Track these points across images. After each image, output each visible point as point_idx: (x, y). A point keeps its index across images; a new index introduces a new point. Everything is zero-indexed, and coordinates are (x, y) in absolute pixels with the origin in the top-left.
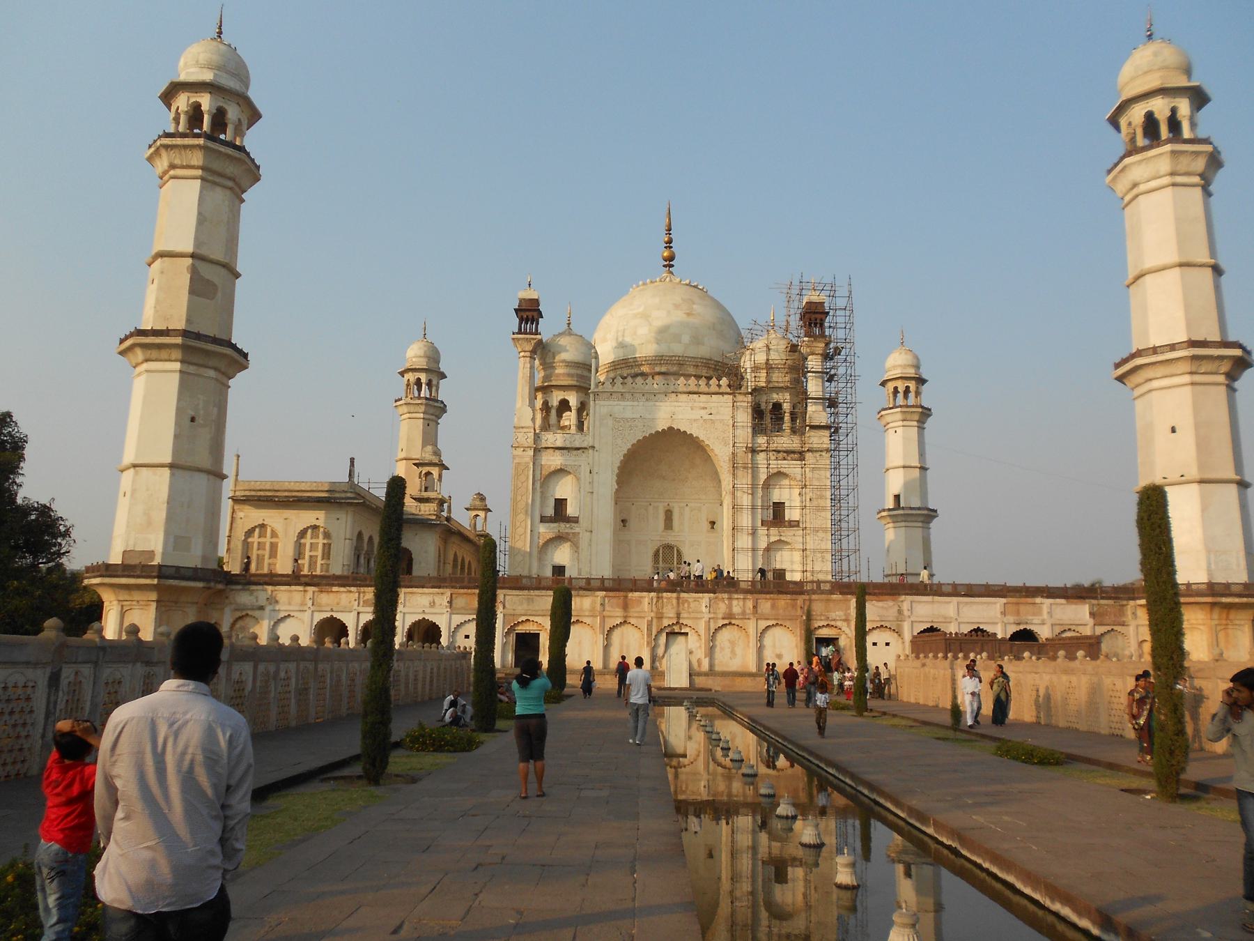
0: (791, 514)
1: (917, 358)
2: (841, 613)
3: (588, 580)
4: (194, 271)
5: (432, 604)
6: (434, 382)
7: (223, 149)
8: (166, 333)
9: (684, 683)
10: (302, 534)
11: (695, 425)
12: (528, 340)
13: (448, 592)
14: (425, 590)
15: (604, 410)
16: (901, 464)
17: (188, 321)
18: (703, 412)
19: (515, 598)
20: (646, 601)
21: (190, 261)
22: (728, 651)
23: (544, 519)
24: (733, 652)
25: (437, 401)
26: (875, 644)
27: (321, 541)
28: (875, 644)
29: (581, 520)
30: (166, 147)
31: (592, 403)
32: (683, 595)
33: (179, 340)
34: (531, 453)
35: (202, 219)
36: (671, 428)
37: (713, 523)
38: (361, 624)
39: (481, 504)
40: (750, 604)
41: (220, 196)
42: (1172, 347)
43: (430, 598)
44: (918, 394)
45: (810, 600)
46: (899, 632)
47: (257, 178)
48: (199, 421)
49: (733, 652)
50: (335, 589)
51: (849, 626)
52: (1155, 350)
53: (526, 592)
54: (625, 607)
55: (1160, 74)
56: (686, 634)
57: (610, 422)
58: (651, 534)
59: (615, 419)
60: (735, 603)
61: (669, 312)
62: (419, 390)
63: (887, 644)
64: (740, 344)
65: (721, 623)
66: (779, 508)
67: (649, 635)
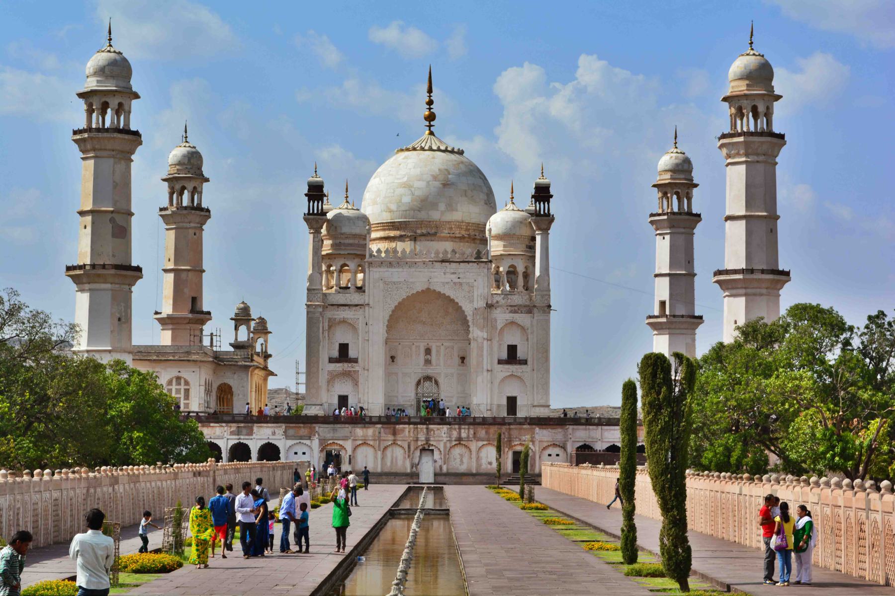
0: (520, 354)
1: (687, 161)
2: (528, 437)
3: (371, 417)
4: (112, 220)
5: (274, 433)
6: (199, 189)
7: (126, 137)
8: (104, 266)
9: (431, 480)
10: (170, 383)
11: (447, 286)
12: (317, 221)
13: (284, 426)
14: (270, 425)
15: (377, 276)
16: (668, 272)
17: (114, 256)
18: (453, 276)
19: (326, 430)
20: (407, 430)
21: (110, 216)
22: (458, 460)
23: (331, 360)
24: (462, 461)
25: (202, 209)
26: (550, 455)
27: (182, 387)
28: (550, 455)
29: (360, 360)
30: (90, 138)
31: (367, 270)
32: (431, 426)
33: (113, 271)
34: (321, 310)
35: (115, 185)
36: (428, 289)
37: (463, 359)
38: (229, 446)
39: (262, 328)
40: (472, 432)
41: (121, 166)
42: (735, 272)
43: (272, 430)
44: (689, 199)
45: (510, 429)
46: (564, 448)
47: (140, 143)
48: (123, 320)
49: (462, 461)
50: (212, 425)
51: (533, 444)
52: (727, 272)
53: (332, 426)
54: (394, 433)
55: (747, 82)
56: (432, 450)
57: (382, 285)
58: (414, 367)
59: (385, 283)
60: (463, 431)
61: (428, 182)
62: (181, 194)
63: (558, 455)
64: (491, 207)
65: (454, 443)
66: (512, 349)
67: (409, 451)
